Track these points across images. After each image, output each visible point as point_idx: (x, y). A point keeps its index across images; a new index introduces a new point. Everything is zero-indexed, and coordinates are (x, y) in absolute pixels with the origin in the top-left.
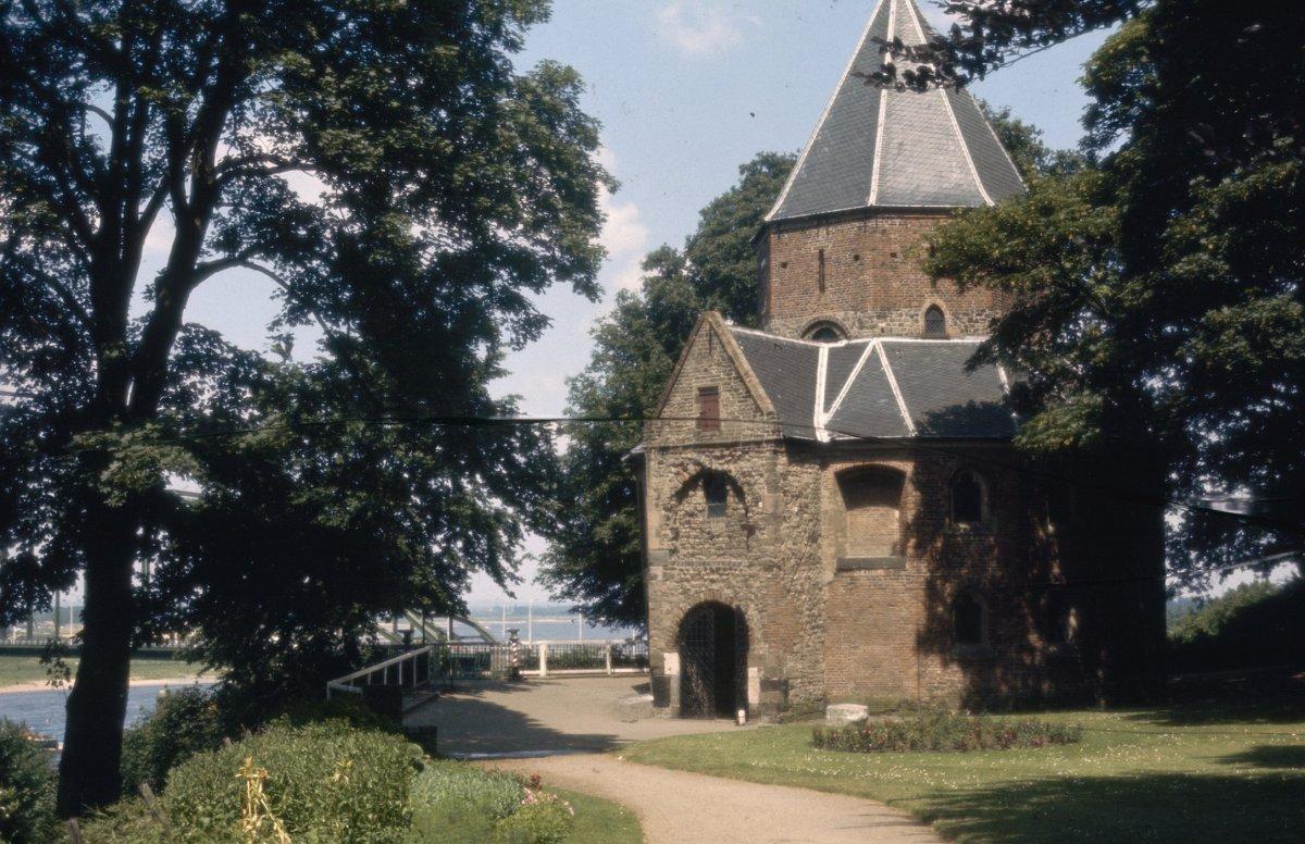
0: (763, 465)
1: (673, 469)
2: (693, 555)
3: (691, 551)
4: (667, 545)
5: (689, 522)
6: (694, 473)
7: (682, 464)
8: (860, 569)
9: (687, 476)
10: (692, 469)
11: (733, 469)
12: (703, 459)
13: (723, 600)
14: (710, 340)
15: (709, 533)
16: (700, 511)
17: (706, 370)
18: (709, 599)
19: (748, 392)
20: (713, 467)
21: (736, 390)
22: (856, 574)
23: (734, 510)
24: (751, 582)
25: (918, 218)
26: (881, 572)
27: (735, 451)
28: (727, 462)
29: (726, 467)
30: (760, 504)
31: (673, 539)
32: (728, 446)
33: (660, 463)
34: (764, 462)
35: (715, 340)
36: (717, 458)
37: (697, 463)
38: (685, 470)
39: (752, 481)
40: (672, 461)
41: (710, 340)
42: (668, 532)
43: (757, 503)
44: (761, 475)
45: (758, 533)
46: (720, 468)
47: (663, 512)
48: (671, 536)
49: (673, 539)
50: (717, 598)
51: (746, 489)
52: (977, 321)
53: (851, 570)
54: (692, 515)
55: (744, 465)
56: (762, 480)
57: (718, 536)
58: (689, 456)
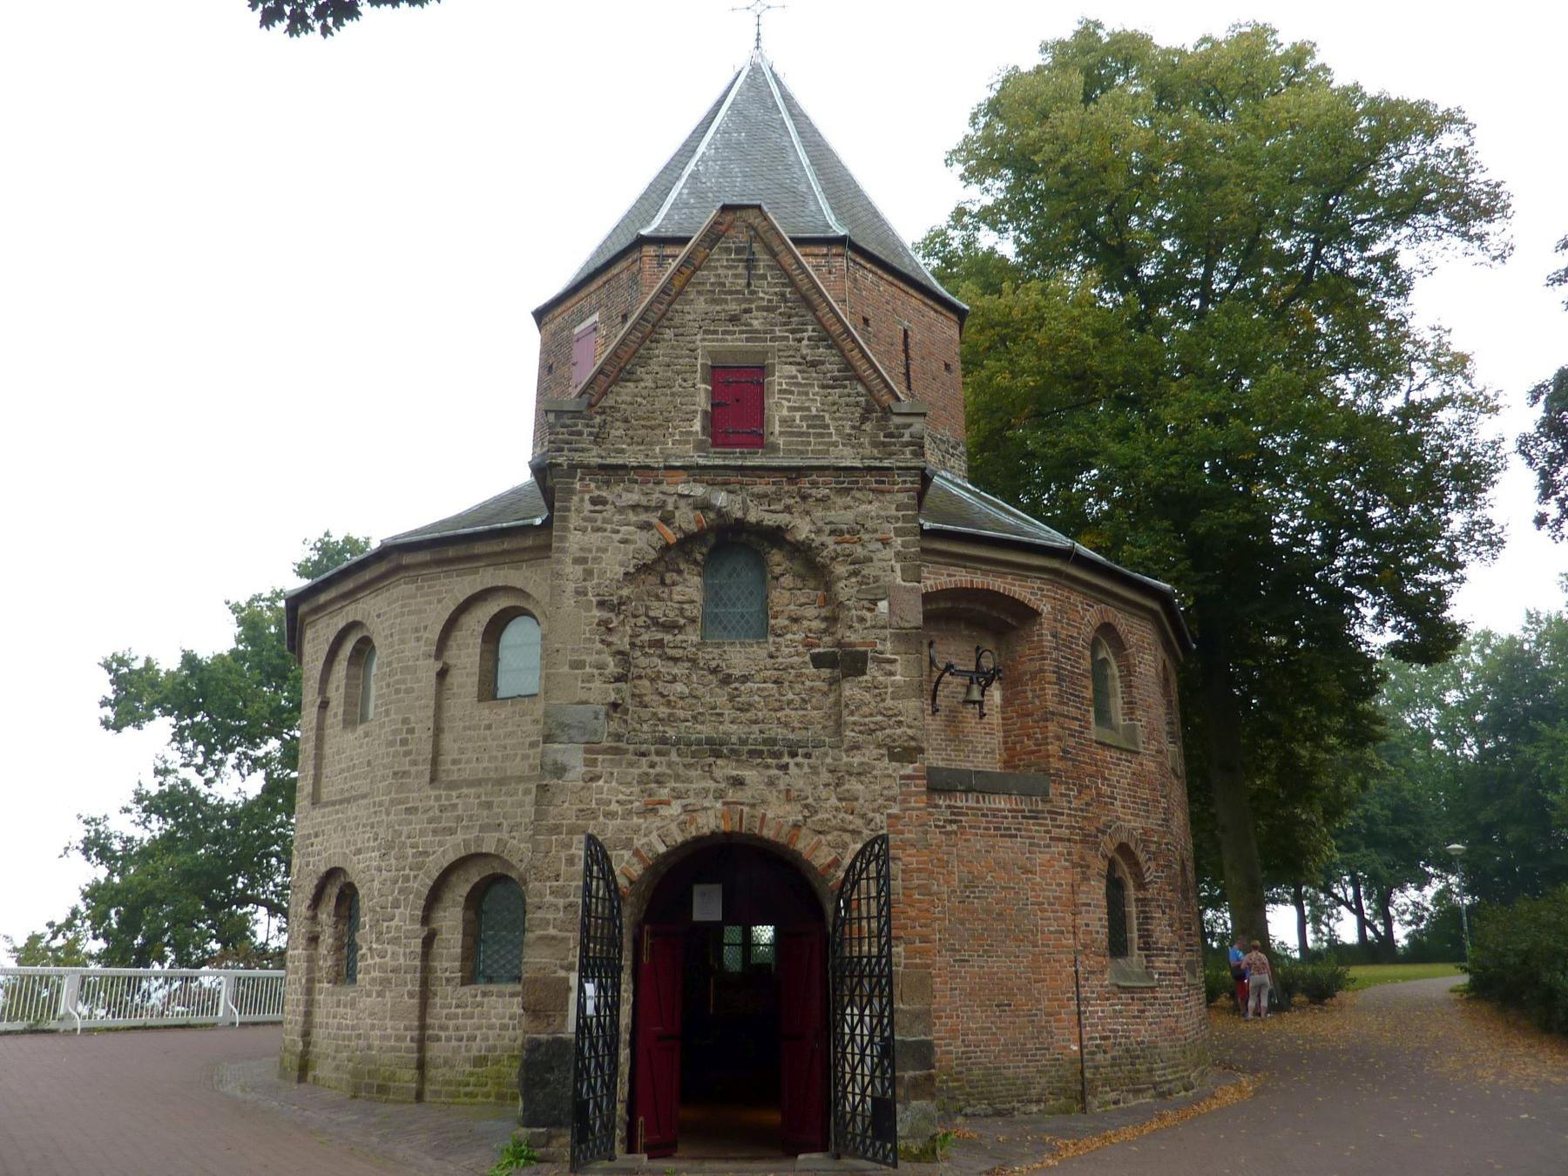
0: (888, 519)
1: (632, 517)
2: (670, 720)
3: (663, 711)
4: (602, 692)
5: (659, 644)
6: (694, 528)
7: (661, 506)
8: (966, 791)
9: (672, 536)
10: (687, 519)
11: (803, 529)
12: (721, 499)
13: (768, 833)
14: (750, 264)
15: (714, 671)
16: (693, 620)
17: (734, 319)
18: (724, 826)
19: (848, 366)
20: (752, 517)
21: (813, 364)
22: (960, 802)
23: (795, 620)
24: (854, 786)
25: (892, 284)
26: (1001, 803)
27: (814, 484)
28: (788, 509)
29: (783, 519)
30: (883, 606)
31: (619, 679)
32: (794, 473)
33: (604, 502)
34: (894, 513)
35: (763, 259)
36: (761, 497)
37: (704, 506)
38: (667, 520)
39: (859, 551)
40: (634, 497)
41: (750, 264)
42: (610, 661)
43: (874, 602)
44: (885, 543)
45: (872, 668)
46: (770, 520)
47: (597, 613)
48: (612, 667)
49: (619, 679)
50: (749, 825)
51: (841, 569)
52: (952, 455)
53: (948, 791)
54: (670, 627)
55: (843, 513)
56: (889, 553)
57: (745, 679)
58: (682, 489)
